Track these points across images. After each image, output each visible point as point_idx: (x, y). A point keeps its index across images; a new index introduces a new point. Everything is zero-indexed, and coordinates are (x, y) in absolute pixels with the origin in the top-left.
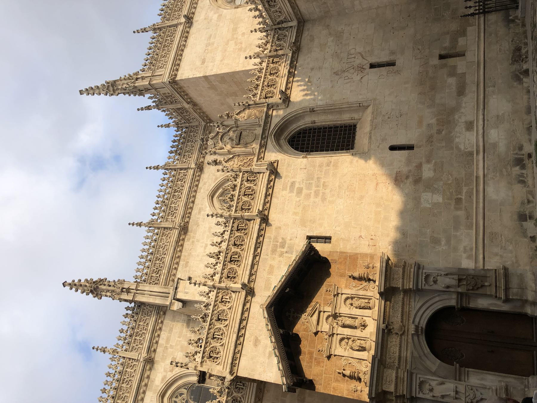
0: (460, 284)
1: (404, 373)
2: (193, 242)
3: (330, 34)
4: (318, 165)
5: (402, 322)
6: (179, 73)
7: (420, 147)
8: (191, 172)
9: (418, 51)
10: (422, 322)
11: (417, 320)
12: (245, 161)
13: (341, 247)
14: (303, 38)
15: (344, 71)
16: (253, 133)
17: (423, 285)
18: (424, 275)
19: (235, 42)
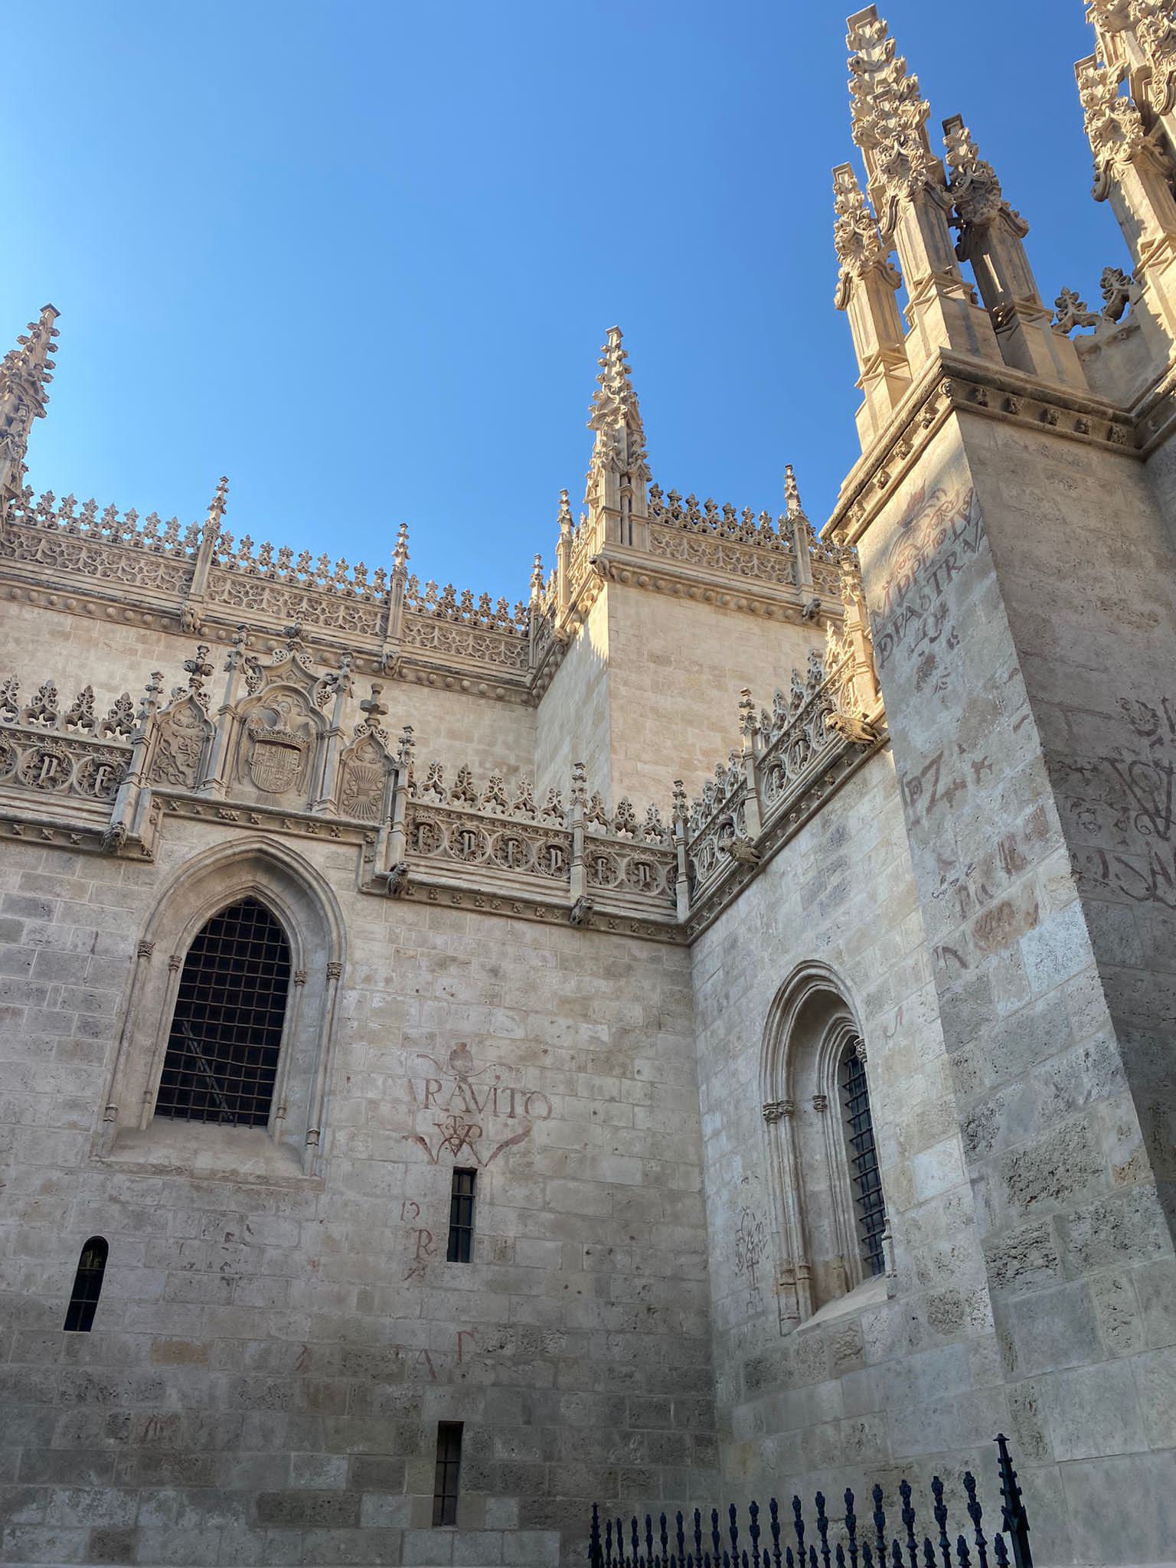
2: (133, 652)
3: (625, 1031)
4: (99, 991)
6: (633, 593)
7: (72, 1353)
8: (370, 643)
9: (492, 1343)
12: (180, 759)
14: (630, 942)
15: (464, 1079)
16: (288, 783)
19: (716, 751)
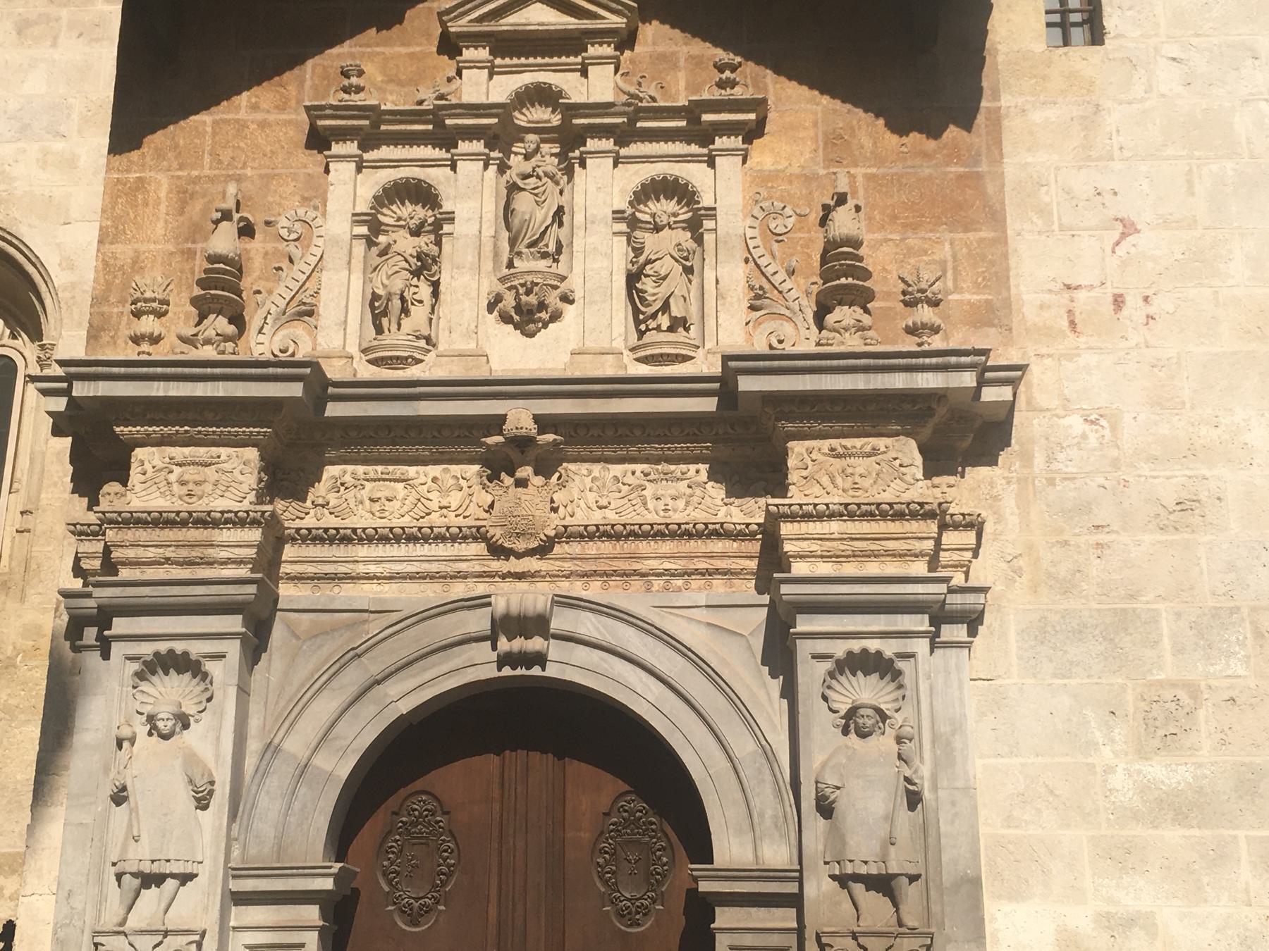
0: (858, 888)
1: (239, 562)
5: (565, 534)
10: (582, 654)
11: (587, 624)
13: (1037, 116)
17: (822, 646)
18: (889, 648)
